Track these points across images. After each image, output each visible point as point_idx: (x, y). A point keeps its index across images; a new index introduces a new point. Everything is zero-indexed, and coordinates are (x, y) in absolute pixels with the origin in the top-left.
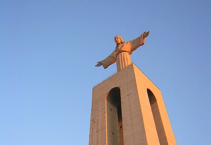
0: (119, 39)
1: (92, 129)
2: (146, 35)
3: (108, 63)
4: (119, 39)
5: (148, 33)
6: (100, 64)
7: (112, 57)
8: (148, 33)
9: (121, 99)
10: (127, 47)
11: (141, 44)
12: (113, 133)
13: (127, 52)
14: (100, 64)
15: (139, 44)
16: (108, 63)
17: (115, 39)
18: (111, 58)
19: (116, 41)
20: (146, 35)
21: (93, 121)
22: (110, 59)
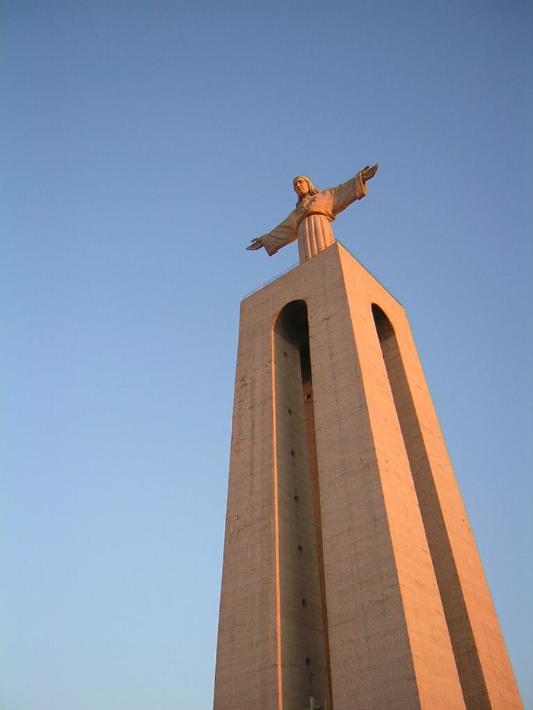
0: (305, 184)
1: (238, 401)
2: (369, 173)
3: (277, 241)
4: (305, 184)
5: (375, 168)
6: (257, 244)
7: (289, 227)
8: (375, 168)
9: (310, 328)
10: (324, 203)
11: (358, 195)
12: (290, 411)
13: (322, 214)
14: (257, 244)
15: (353, 195)
16: (277, 241)
17: (295, 185)
18: (287, 230)
19: (297, 189)
20: (369, 173)
21: (242, 381)
22: (283, 232)
